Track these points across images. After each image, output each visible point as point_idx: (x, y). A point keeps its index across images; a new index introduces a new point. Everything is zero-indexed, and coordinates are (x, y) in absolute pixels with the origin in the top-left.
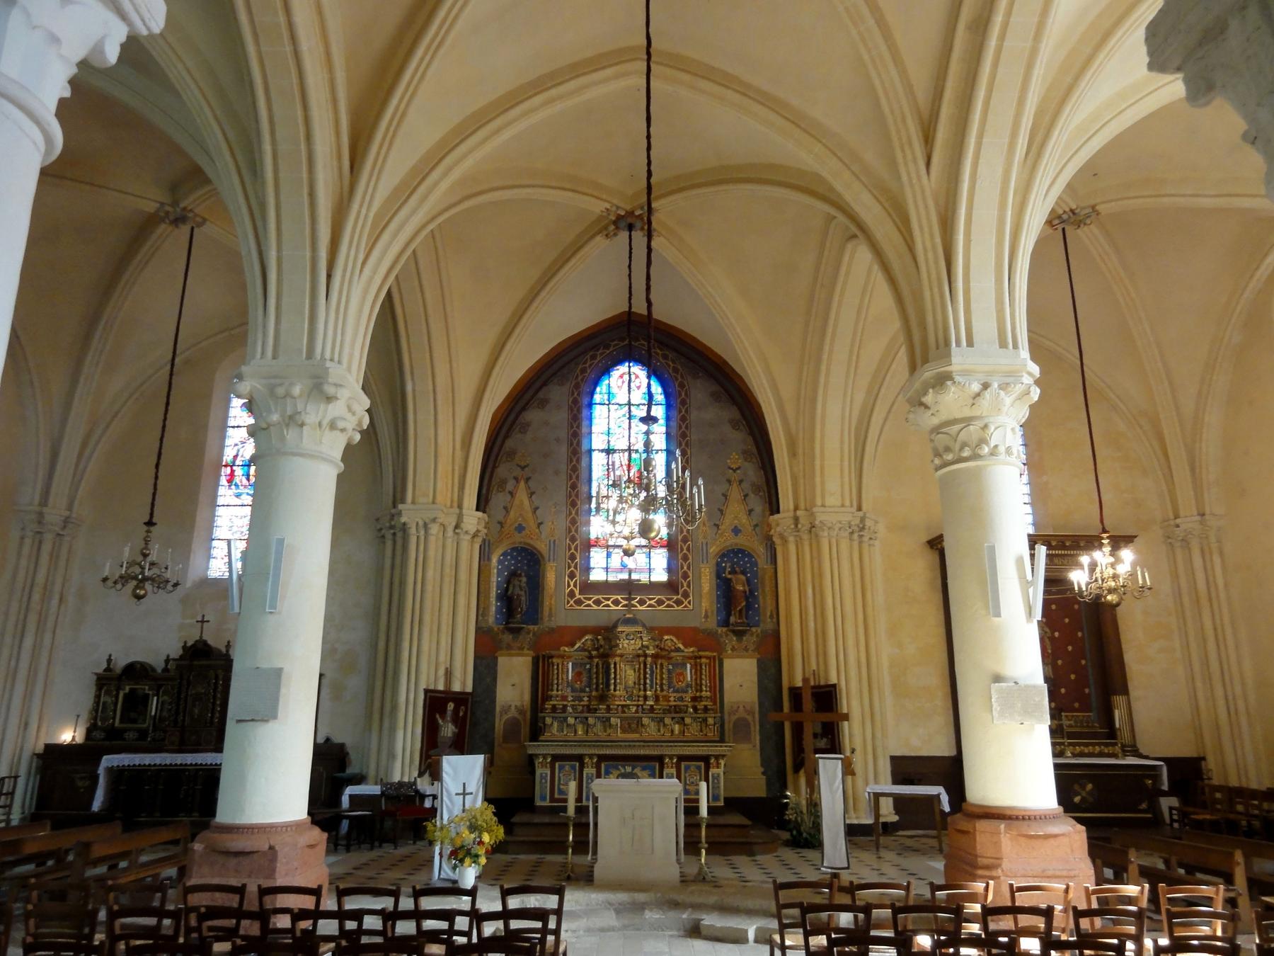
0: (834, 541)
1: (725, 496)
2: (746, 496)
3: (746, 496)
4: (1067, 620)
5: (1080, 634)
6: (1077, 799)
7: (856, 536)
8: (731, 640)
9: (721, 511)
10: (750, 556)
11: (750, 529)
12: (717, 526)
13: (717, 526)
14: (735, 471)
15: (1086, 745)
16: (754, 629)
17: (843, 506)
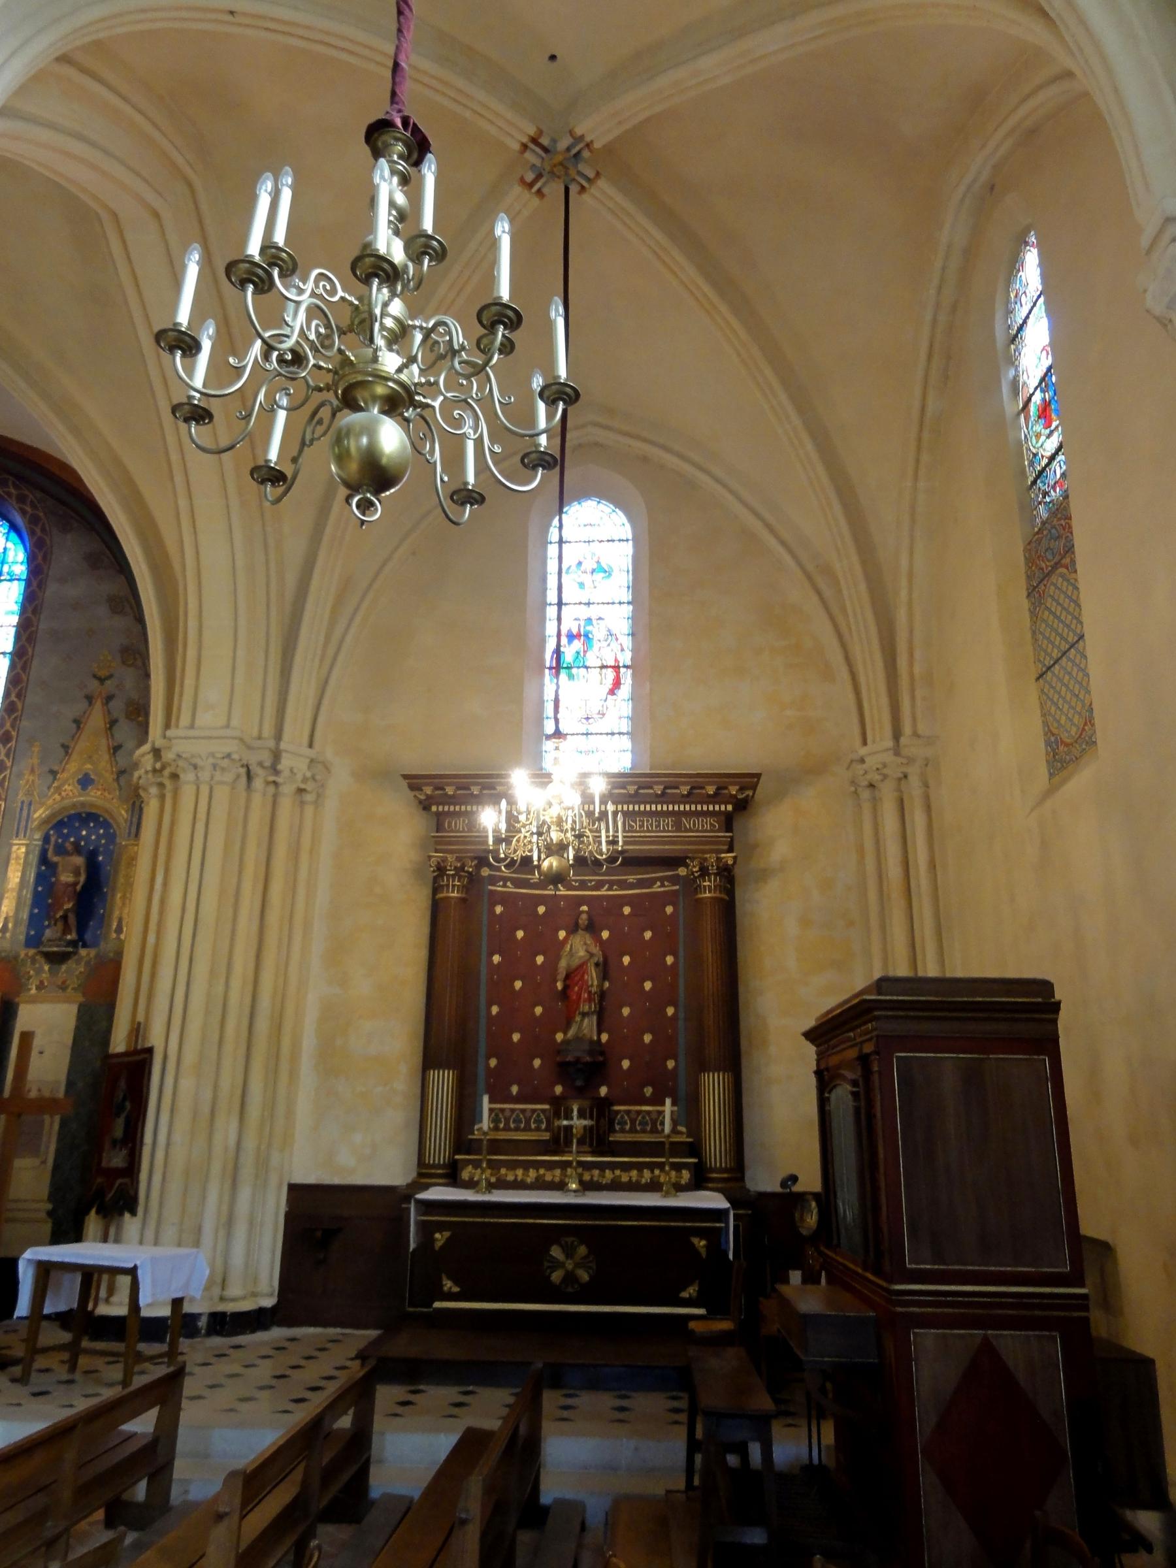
0: (205, 790)
1: (77, 722)
2: (113, 723)
3: (113, 723)
4: (648, 935)
5: (670, 960)
6: (556, 1276)
7: (258, 783)
8: (39, 971)
9: (65, 747)
10: (106, 825)
11: (110, 777)
12: (53, 773)
13: (53, 773)
14: (102, 680)
15: (626, 1167)
16: (83, 952)
17: (228, 726)
